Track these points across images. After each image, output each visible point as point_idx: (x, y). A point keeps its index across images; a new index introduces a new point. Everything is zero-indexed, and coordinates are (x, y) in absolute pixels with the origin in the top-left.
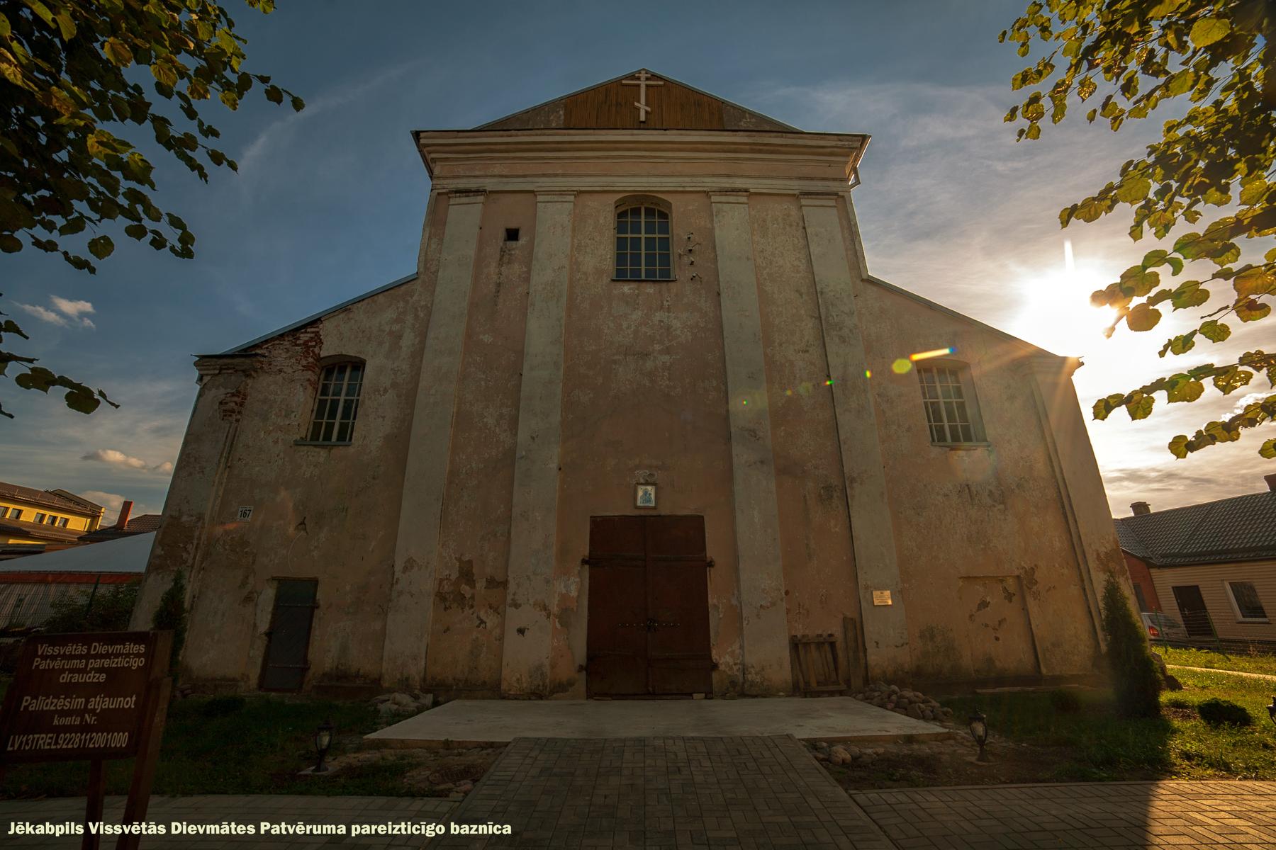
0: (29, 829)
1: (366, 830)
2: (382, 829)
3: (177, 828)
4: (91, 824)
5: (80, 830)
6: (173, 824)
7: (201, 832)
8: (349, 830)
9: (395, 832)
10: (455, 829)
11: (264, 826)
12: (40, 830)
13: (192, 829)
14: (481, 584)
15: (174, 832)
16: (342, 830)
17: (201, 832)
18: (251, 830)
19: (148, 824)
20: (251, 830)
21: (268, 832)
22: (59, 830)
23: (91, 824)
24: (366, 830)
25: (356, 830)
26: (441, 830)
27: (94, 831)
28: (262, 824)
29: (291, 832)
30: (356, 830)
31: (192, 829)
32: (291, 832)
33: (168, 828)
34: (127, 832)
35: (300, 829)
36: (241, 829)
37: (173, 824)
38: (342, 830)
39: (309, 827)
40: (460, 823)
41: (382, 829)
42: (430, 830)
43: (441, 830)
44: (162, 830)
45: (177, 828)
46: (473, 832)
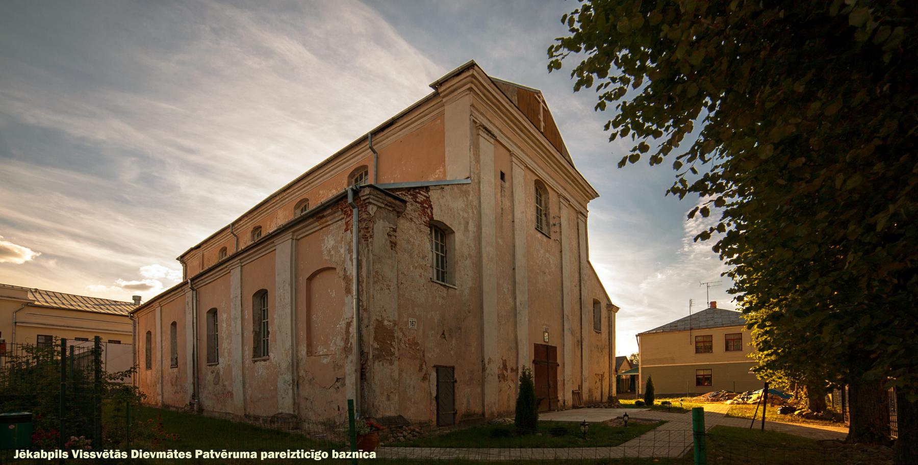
0: (29, 455)
1: (272, 455)
2: (283, 455)
3: (136, 454)
5: (66, 455)
6: (133, 451)
7: (153, 457)
8: (259, 456)
10: (335, 454)
11: (198, 453)
12: (37, 455)
13: (146, 455)
14: (509, 370)
15: (133, 457)
16: (254, 455)
17: (153, 457)
18: (189, 455)
19: (114, 451)
20: (189, 455)
21: (201, 457)
22: (50, 455)
24: (272, 455)
25: (264, 455)
26: (325, 455)
27: (75, 456)
28: (197, 451)
29: (218, 457)
30: (264, 455)
31: (146, 455)
32: (218, 457)
33: (129, 454)
34: (99, 457)
35: (224, 455)
36: (181, 455)
37: (133, 451)
38: (254, 455)
39: (230, 454)
40: (338, 451)
41: (283, 455)
42: (318, 456)
43: (325, 455)
44: (125, 455)
45: (136, 454)
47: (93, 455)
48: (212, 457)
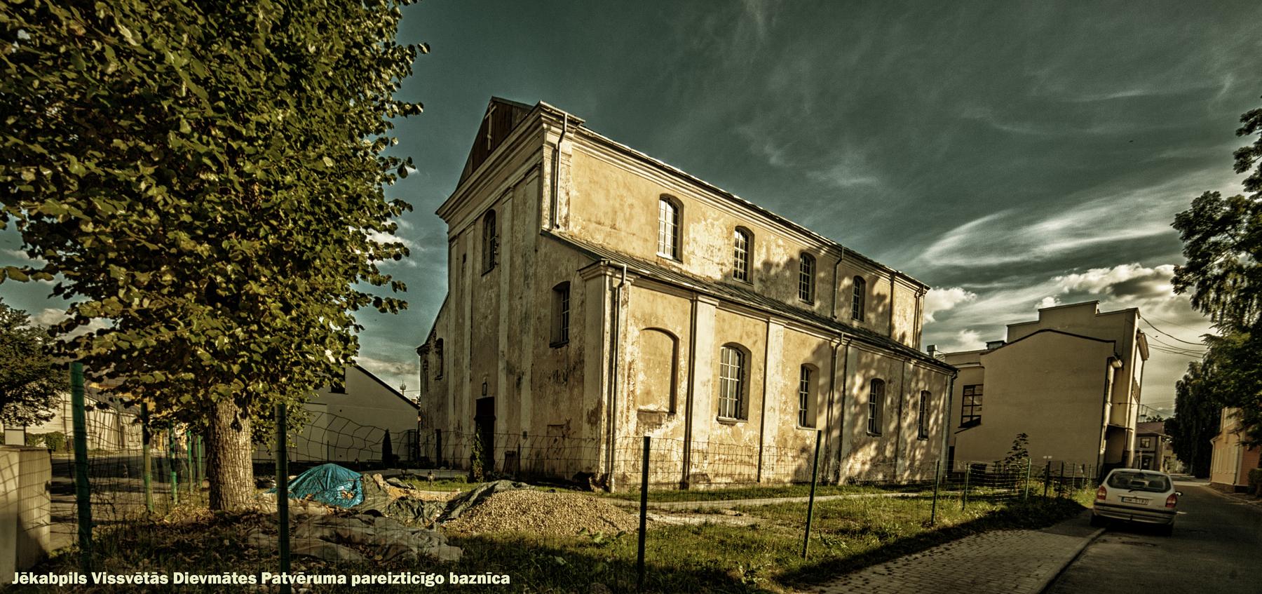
0: (33, 579)
3: (179, 578)
4: (94, 574)
5: (83, 580)
6: (176, 574)
7: (203, 582)
8: (349, 580)
9: (395, 582)
10: (454, 579)
12: (44, 580)
13: (194, 579)
15: (176, 582)
21: (269, 582)
23: (94, 574)
24: (367, 580)
26: (440, 579)
27: (97, 581)
31: (194, 579)
36: (243, 580)
37: (176, 574)
38: (343, 580)
40: (459, 573)
42: (430, 580)
43: (440, 579)
44: (164, 580)
45: (179, 578)
46: (472, 582)
47: (121, 580)
48: (285, 582)
